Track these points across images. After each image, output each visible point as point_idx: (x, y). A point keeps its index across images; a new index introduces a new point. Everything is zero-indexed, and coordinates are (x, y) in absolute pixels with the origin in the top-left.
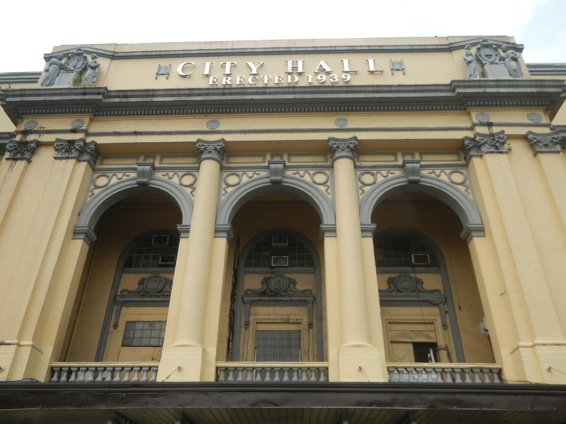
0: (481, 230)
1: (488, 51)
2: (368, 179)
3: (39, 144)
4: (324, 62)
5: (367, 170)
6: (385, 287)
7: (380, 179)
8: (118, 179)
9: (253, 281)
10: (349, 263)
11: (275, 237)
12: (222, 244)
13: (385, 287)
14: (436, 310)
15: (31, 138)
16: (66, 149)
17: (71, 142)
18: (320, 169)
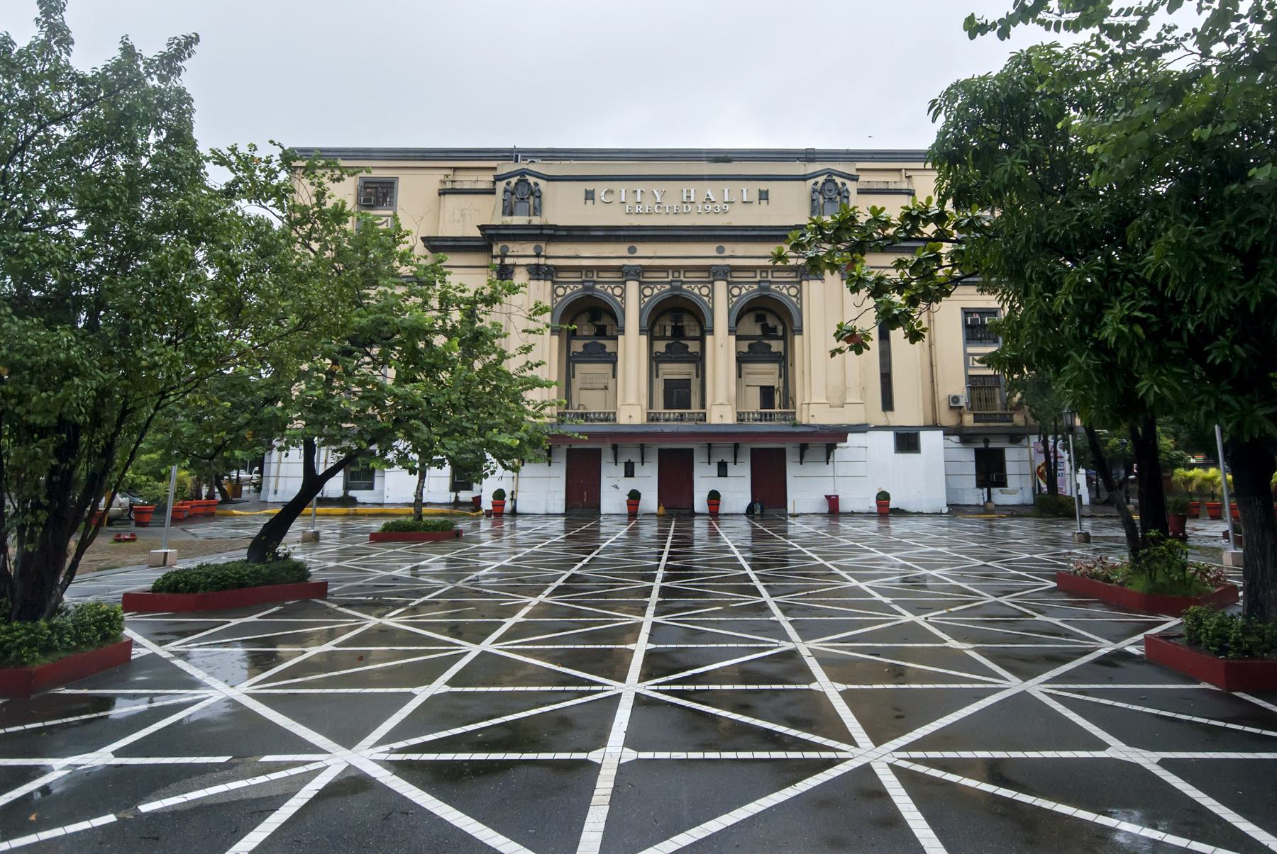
0: (800, 332)
1: (830, 186)
2: (736, 291)
3: (515, 265)
4: (710, 189)
5: (736, 284)
6: (746, 350)
7: (744, 291)
8: (570, 290)
9: (660, 346)
10: (721, 349)
11: (677, 322)
12: (644, 338)
13: (746, 350)
14: (777, 366)
15: (508, 261)
16: (537, 272)
17: (538, 266)
18: (704, 284)
